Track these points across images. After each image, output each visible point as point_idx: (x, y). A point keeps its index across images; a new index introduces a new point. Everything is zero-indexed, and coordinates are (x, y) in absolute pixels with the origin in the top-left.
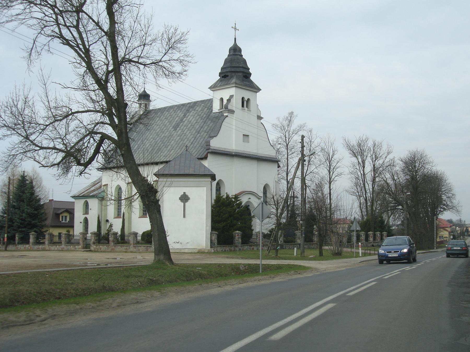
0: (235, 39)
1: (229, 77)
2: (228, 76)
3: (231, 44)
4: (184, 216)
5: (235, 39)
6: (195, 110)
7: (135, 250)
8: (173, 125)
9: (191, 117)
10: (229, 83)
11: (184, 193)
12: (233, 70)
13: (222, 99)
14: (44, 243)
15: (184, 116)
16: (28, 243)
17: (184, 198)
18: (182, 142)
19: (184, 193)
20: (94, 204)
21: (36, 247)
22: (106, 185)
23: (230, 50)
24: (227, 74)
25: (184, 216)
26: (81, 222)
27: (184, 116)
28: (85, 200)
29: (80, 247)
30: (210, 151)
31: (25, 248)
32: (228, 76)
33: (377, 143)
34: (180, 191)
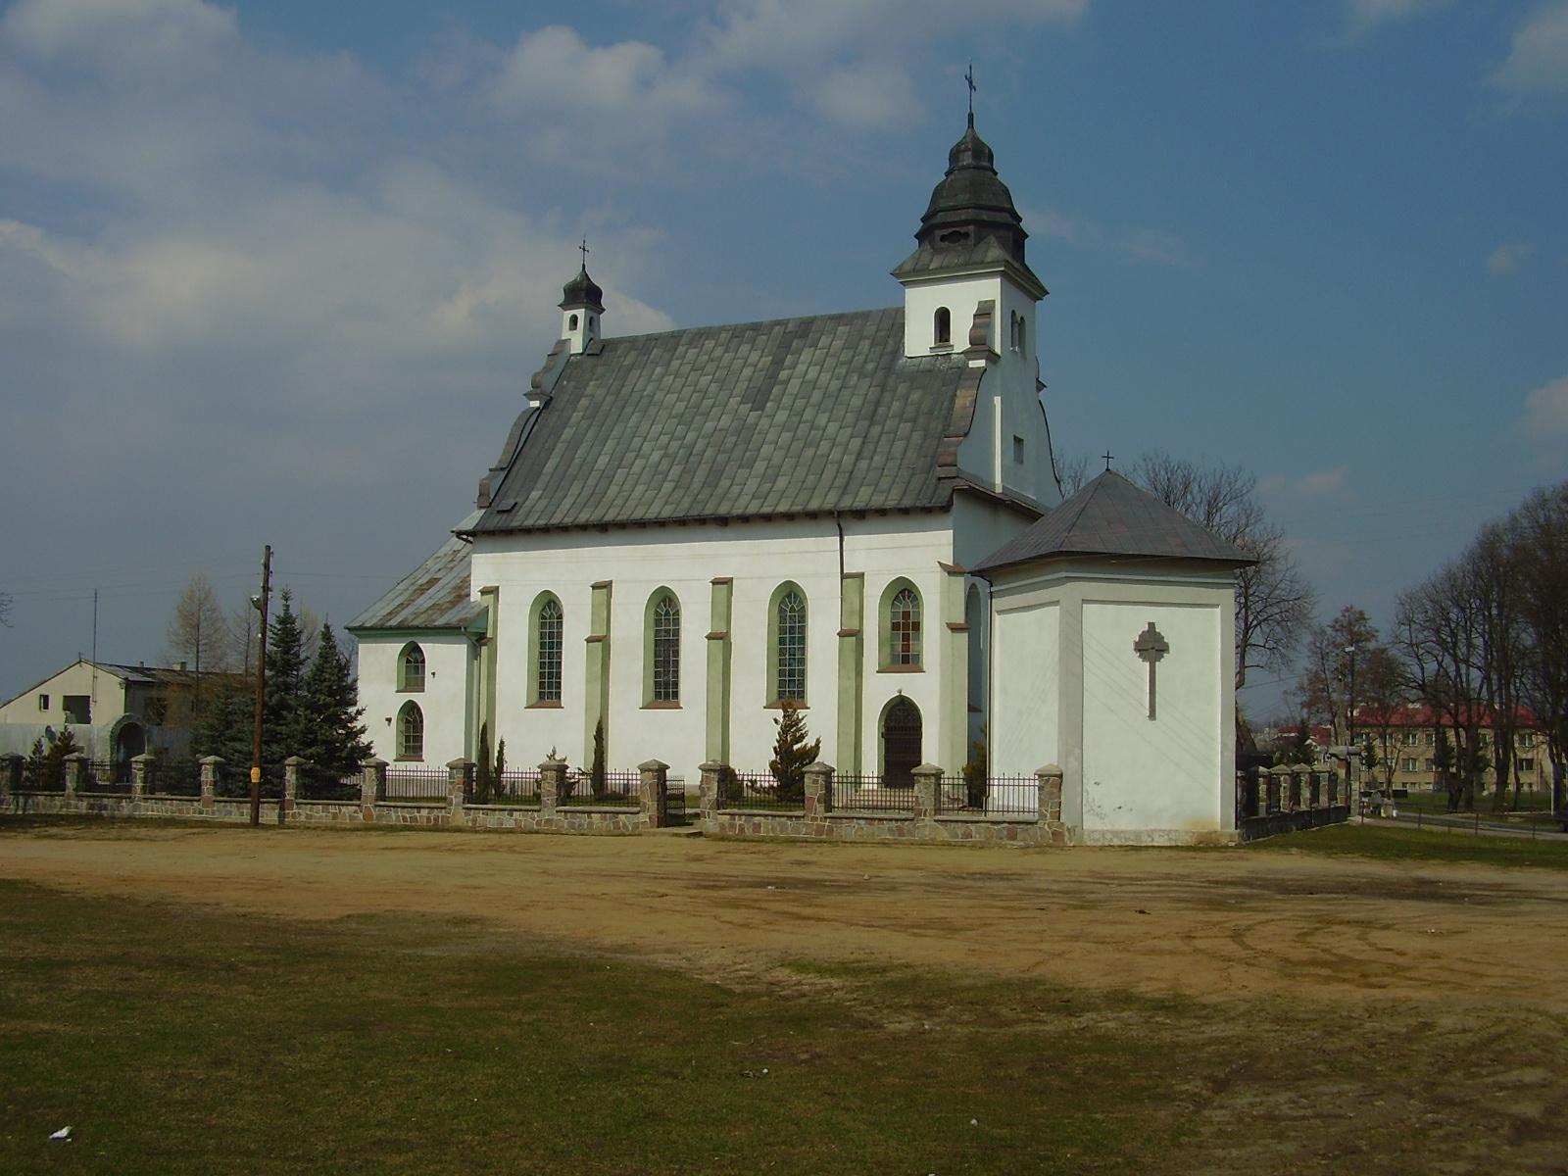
0: (971, 116)
1: (971, 241)
2: (966, 235)
3: (957, 133)
4: (1152, 715)
5: (971, 116)
6: (815, 345)
7: (943, 834)
8: (741, 387)
9: (805, 365)
10: (977, 257)
11: (1152, 625)
12: (963, 217)
13: (943, 318)
14: (354, 794)
15: (778, 363)
16: (61, 787)
17: (1151, 646)
18: (809, 452)
19: (1152, 625)
20: (445, 659)
21: (319, 812)
22: (491, 591)
23: (955, 155)
24: (962, 230)
25: (1152, 715)
26: (389, 720)
27: (778, 363)
28: (410, 639)
29: (643, 817)
30: (961, 484)
31: (474, 821)
32: (966, 235)
33: (1256, 508)
34: (1134, 620)
